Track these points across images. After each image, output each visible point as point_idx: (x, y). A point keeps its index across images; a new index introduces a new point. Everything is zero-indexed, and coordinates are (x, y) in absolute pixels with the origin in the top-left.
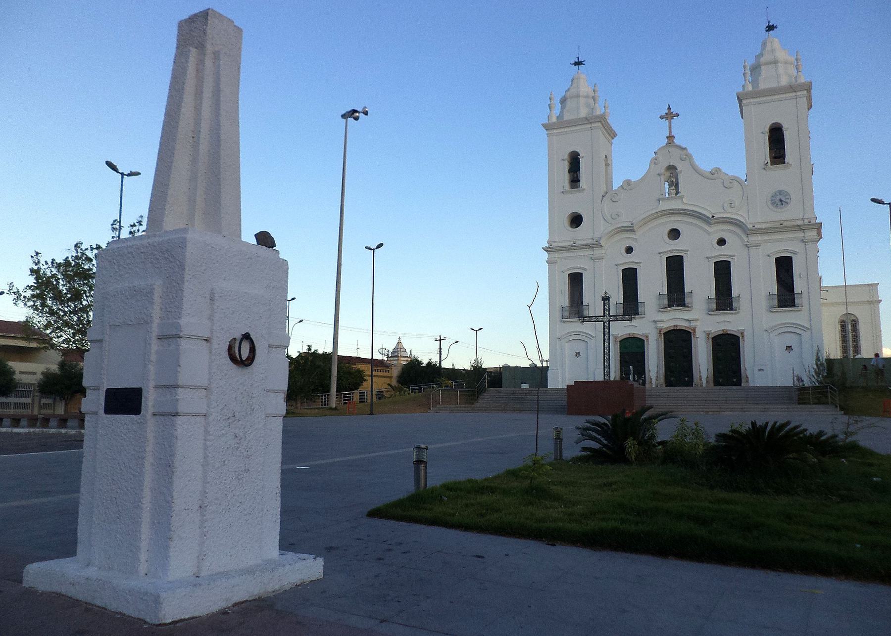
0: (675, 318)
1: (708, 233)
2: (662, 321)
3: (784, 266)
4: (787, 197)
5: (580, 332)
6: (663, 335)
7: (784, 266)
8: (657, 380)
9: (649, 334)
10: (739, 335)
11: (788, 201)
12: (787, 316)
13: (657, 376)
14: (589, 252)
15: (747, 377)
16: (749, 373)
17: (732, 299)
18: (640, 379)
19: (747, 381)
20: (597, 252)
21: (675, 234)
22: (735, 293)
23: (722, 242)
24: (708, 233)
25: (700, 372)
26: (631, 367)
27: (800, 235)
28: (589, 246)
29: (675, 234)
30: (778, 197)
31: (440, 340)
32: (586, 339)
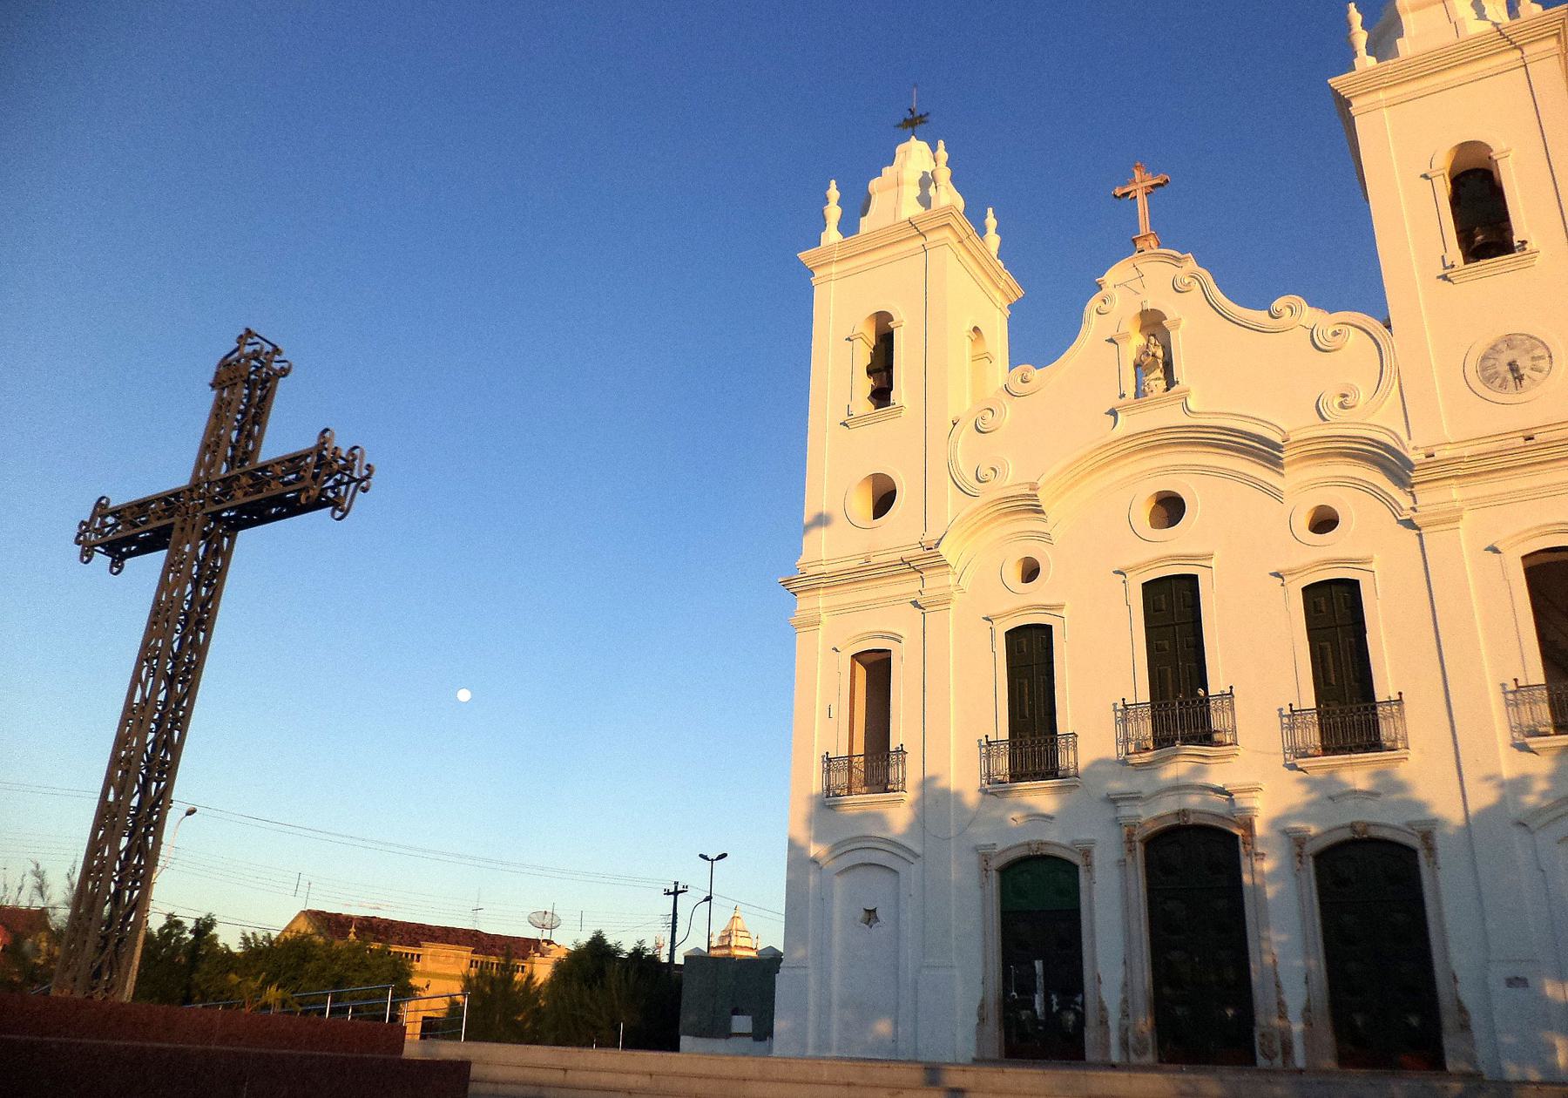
1: (1277, 495)
4: (1538, 352)
6: (1140, 848)
8: (1125, 1015)
9: (1093, 842)
10: (1415, 842)
11: (1544, 364)
13: (1125, 1001)
14: (909, 586)
16: (1468, 996)
17: (1374, 708)
18: (1069, 1009)
20: (934, 583)
21: (1170, 508)
22: (1384, 689)
23: (1324, 522)
24: (1277, 495)
25: (1278, 986)
26: (1038, 965)
28: (910, 566)
29: (1170, 508)
30: (1507, 357)
32: (895, 864)
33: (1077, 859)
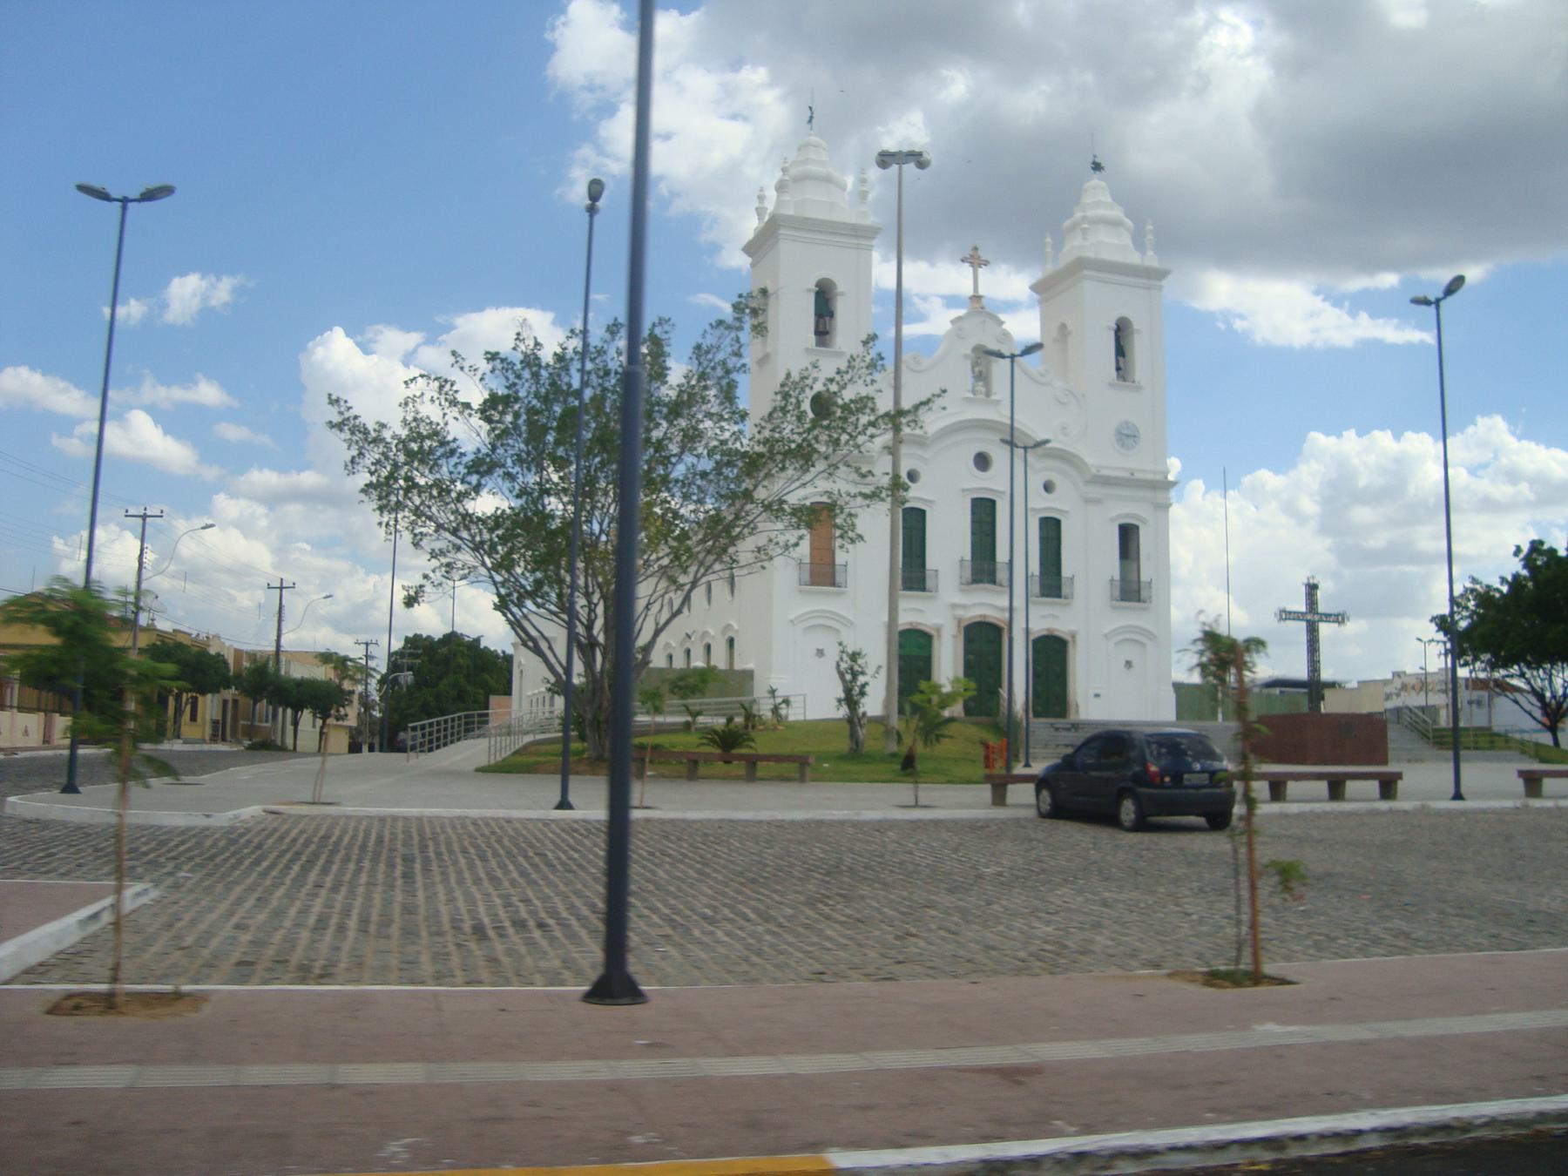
0: (986, 604)
2: (964, 607)
3: (1128, 535)
5: (813, 612)
7: (1128, 535)
12: (1130, 617)
15: (1077, 706)
19: (1077, 711)
21: (982, 461)
27: (1149, 494)
31: (281, 588)
33: (933, 632)
